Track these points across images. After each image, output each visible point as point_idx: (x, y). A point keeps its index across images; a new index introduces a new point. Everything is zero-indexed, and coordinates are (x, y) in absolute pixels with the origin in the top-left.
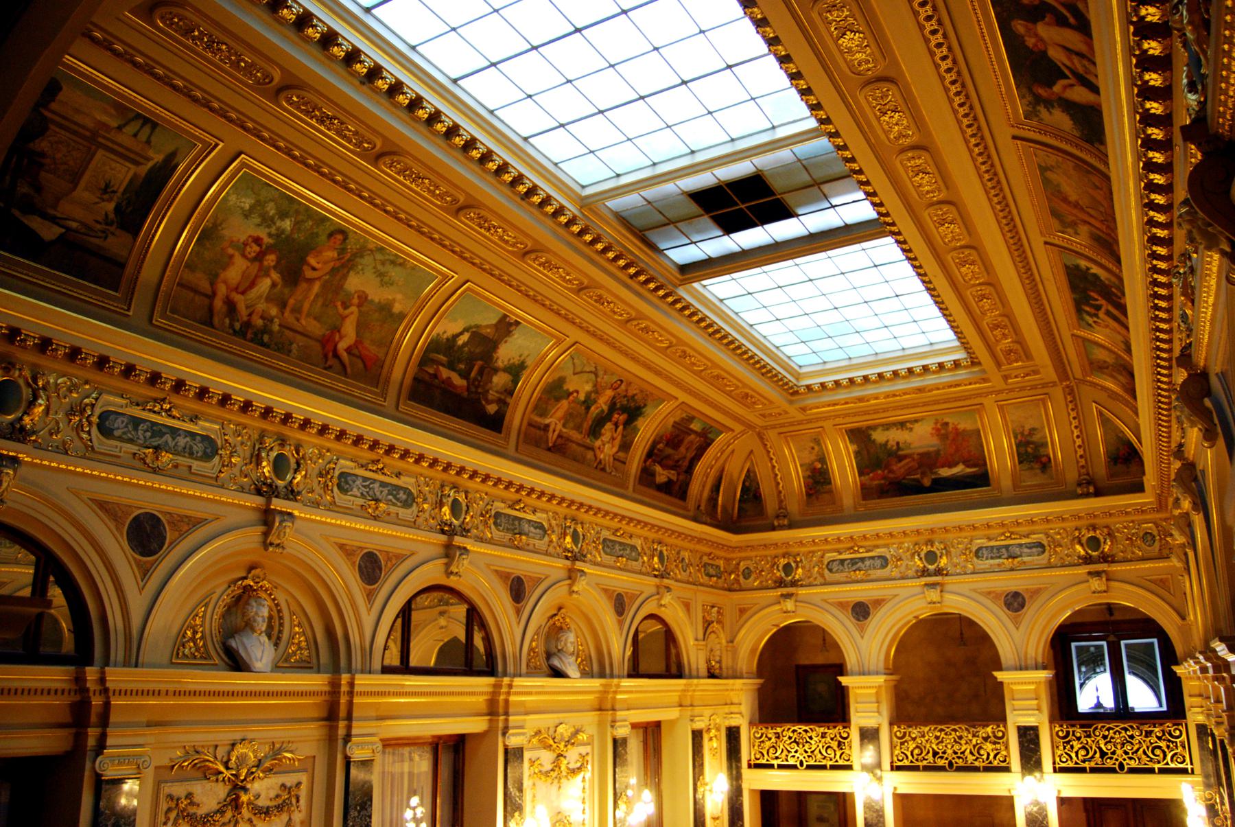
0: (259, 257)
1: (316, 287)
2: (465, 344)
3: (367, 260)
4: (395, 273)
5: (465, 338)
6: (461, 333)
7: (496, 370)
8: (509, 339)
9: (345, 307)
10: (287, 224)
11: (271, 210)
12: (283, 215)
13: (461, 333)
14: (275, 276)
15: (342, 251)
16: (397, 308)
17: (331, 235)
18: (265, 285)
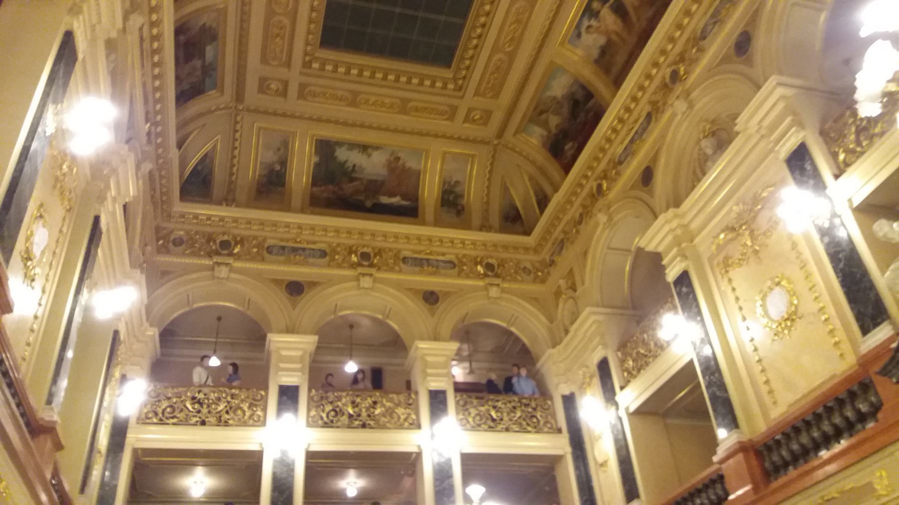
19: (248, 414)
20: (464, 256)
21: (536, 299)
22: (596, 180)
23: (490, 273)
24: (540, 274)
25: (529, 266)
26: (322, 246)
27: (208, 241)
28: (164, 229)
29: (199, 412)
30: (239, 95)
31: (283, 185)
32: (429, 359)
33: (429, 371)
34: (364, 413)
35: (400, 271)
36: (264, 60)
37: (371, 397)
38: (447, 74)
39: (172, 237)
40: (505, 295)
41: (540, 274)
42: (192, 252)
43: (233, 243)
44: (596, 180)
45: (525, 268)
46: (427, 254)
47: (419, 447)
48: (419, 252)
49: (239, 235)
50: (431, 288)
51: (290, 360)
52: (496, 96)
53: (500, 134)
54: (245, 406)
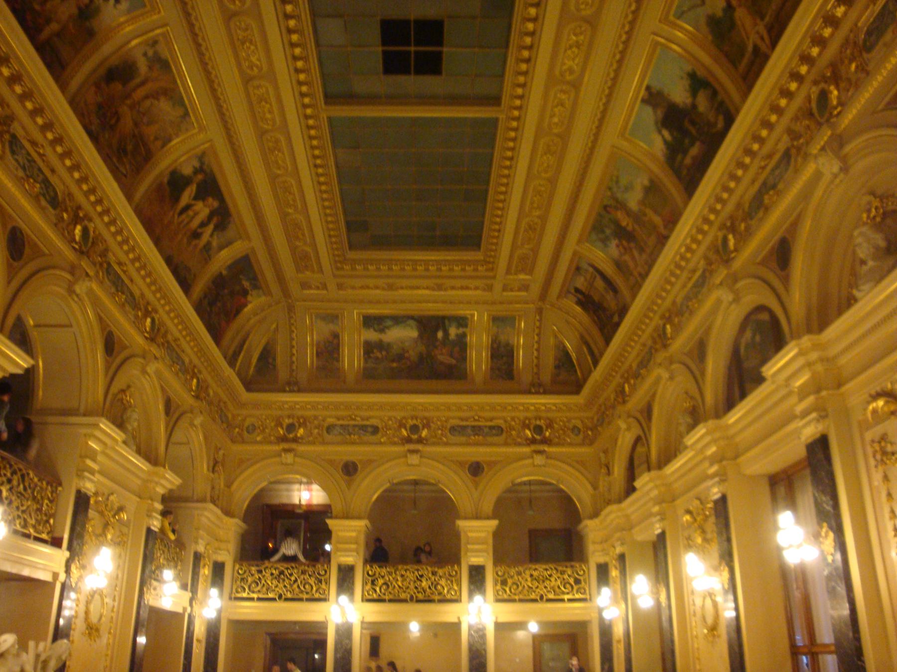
0: (625, 249)
1: (637, 227)
2: (671, 134)
3: (619, 195)
4: (624, 181)
5: (666, 133)
6: (663, 136)
7: (694, 106)
8: (666, 91)
9: (645, 215)
10: (608, 232)
11: (601, 236)
12: (603, 232)
13: (663, 136)
14: (632, 245)
15: (617, 208)
16: (646, 182)
17: (608, 212)
18: (636, 253)
19: (314, 589)
20: (513, 419)
21: (582, 463)
22: (815, 83)
23: (538, 437)
24: (590, 433)
25: (579, 424)
26: (374, 422)
27: (276, 426)
28: (238, 415)
29: (276, 586)
30: (286, 293)
31: (338, 360)
32: (470, 534)
33: (469, 546)
34: (412, 586)
35: (447, 444)
36: (298, 270)
37: (418, 570)
38: (479, 256)
39: (247, 424)
40: (549, 461)
41: (590, 433)
42: (264, 438)
43: (297, 425)
44: (815, 83)
45: (575, 427)
46: (475, 420)
47: (459, 618)
48: (466, 420)
49: (302, 417)
50: (479, 459)
51: (348, 541)
52: (531, 272)
53: (543, 297)
54: (312, 581)
